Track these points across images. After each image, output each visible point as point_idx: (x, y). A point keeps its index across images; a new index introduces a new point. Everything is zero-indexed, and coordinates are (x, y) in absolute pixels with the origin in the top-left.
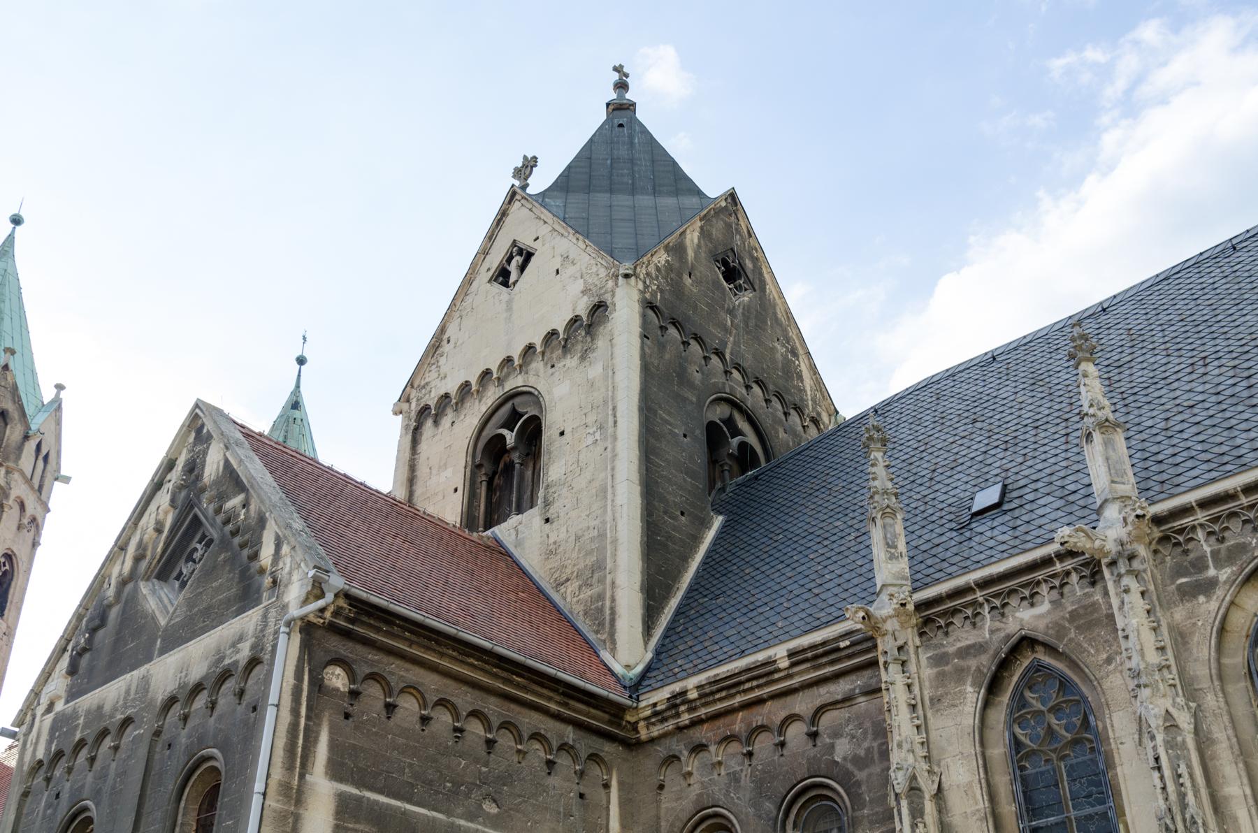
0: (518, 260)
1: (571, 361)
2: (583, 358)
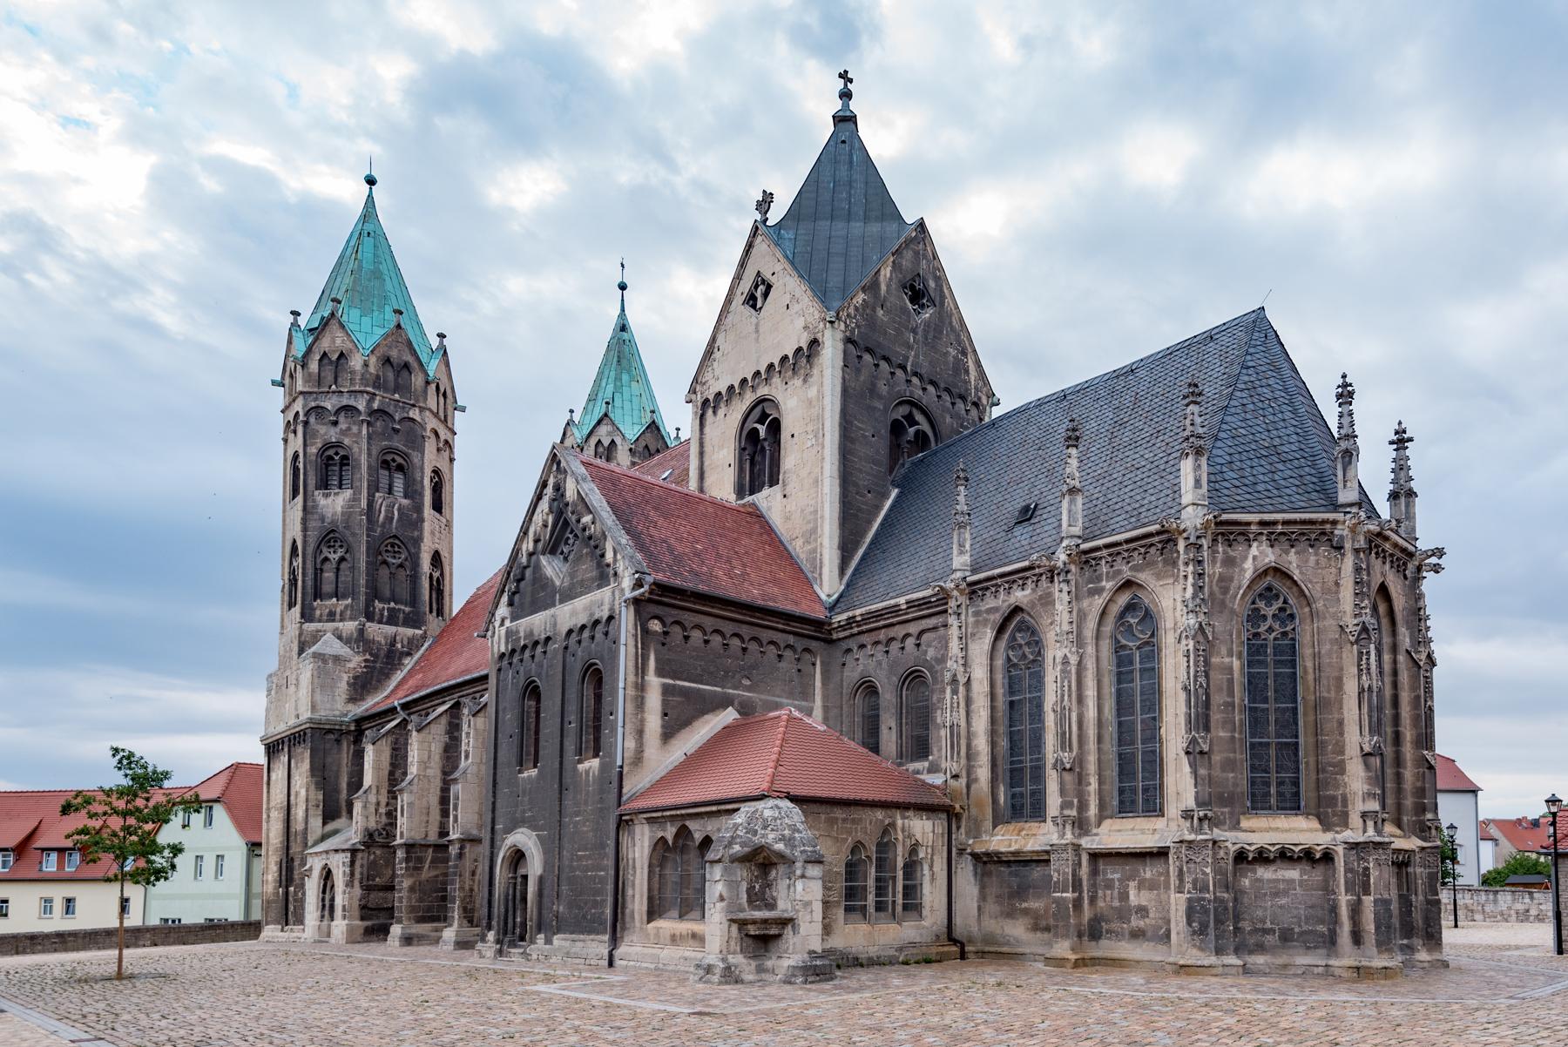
0: (762, 288)
1: (798, 382)
2: (805, 381)
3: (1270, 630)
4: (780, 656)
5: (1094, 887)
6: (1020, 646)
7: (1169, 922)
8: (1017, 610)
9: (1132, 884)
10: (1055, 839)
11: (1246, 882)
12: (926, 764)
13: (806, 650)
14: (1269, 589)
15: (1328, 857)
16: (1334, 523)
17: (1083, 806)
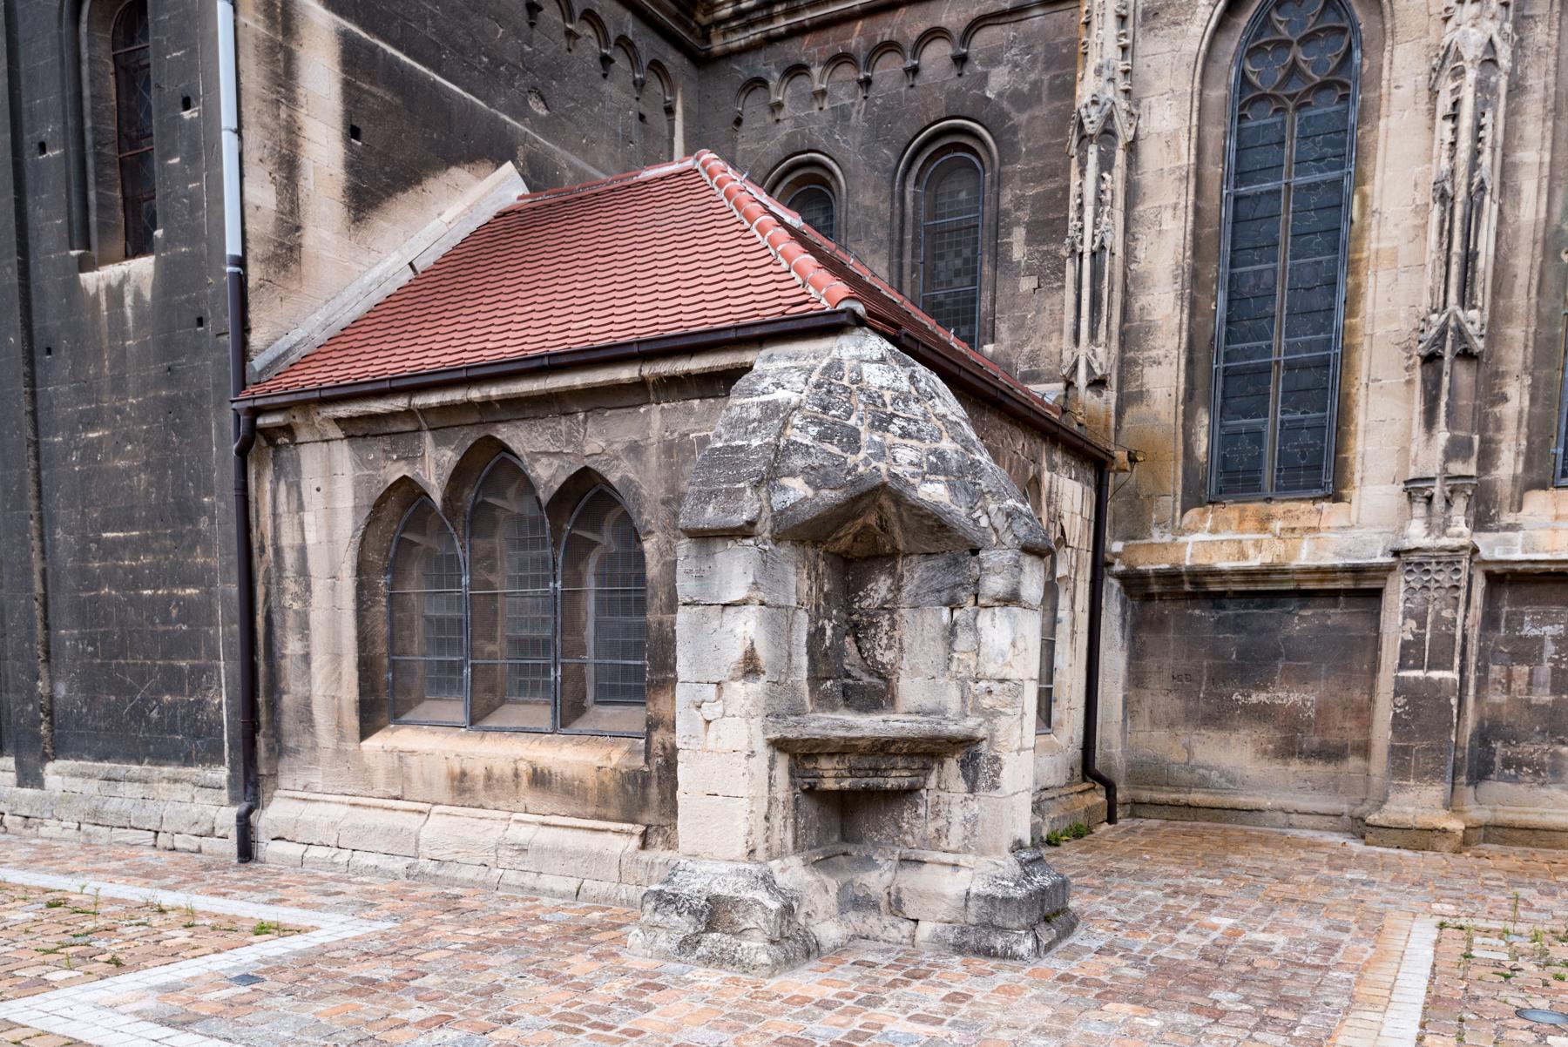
6: (1287, 44)
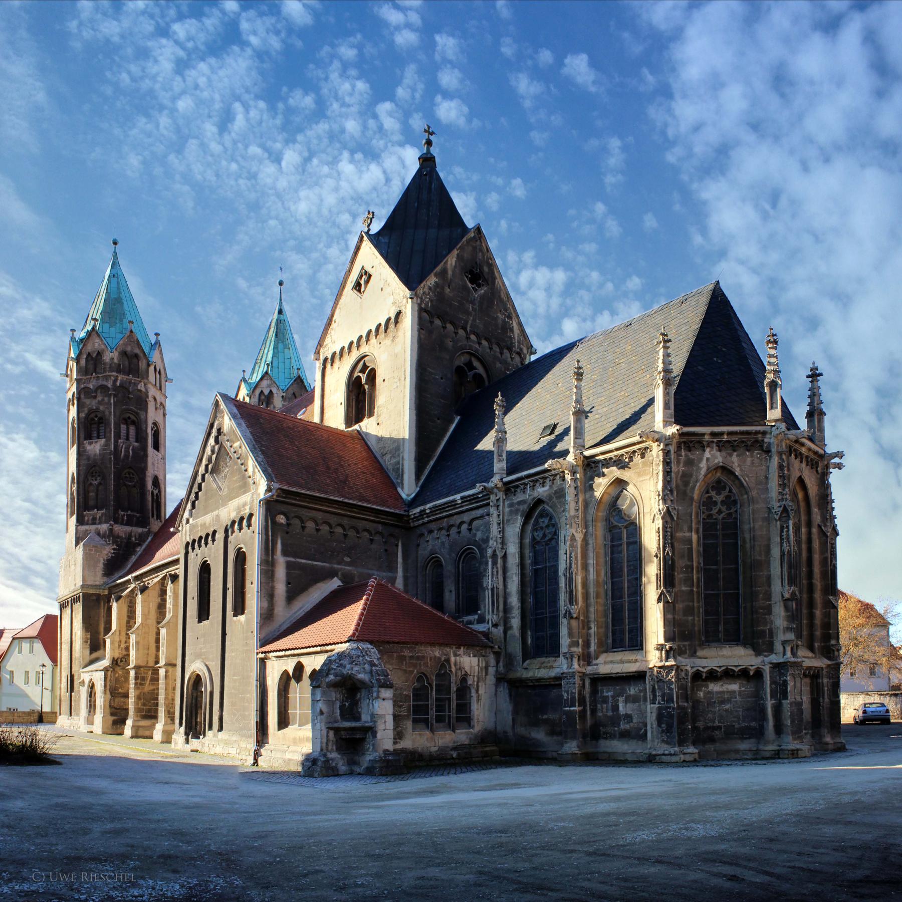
3: (720, 512)
4: (372, 540)
5: (594, 702)
6: (542, 528)
7: (646, 725)
8: (539, 502)
9: (621, 699)
10: (565, 668)
11: (701, 694)
12: (476, 617)
13: (391, 535)
14: (719, 481)
15: (759, 674)
16: (764, 433)
17: (587, 644)
